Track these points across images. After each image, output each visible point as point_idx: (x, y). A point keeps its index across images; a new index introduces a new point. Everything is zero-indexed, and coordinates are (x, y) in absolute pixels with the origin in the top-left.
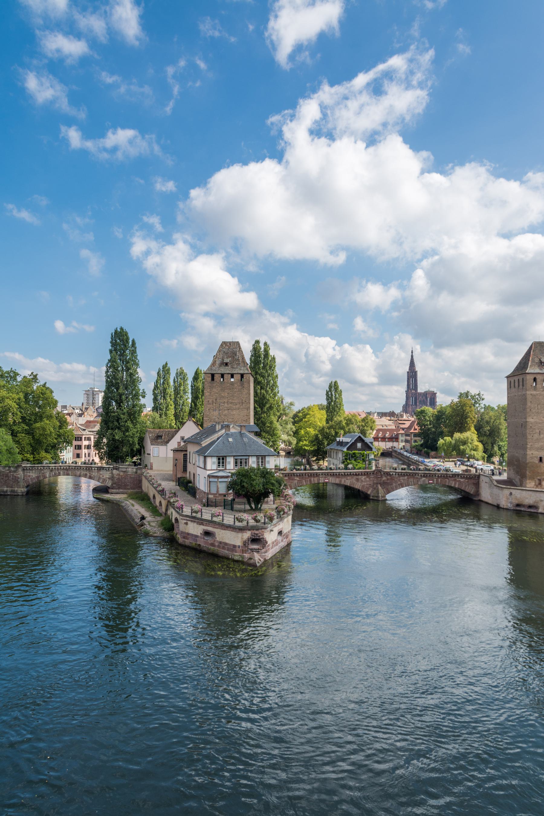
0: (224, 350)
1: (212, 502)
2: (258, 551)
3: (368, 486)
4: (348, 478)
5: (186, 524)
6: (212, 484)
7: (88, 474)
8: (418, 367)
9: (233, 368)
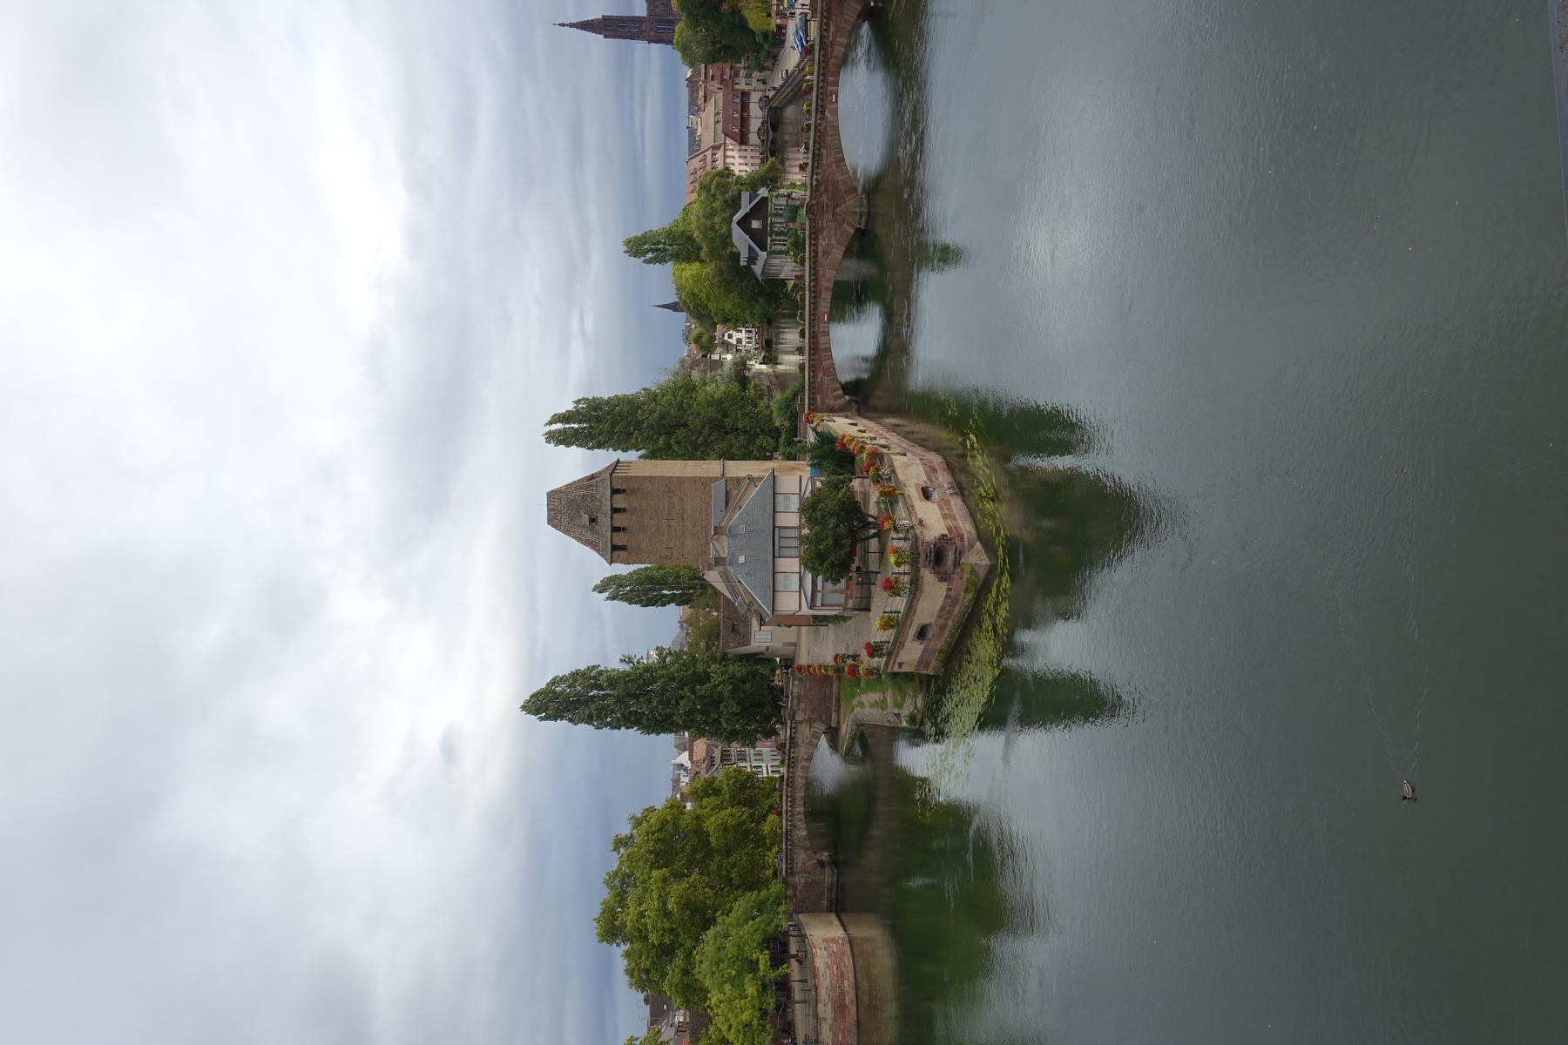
0: (564, 522)
1: (861, 602)
2: (959, 554)
3: (838, 234)
4: (821, 273)
5: (900, 665)
6: (826, 602)
7: (802, 763)
8: (595, 14)
9: (599, 510)
